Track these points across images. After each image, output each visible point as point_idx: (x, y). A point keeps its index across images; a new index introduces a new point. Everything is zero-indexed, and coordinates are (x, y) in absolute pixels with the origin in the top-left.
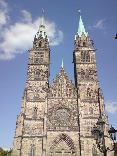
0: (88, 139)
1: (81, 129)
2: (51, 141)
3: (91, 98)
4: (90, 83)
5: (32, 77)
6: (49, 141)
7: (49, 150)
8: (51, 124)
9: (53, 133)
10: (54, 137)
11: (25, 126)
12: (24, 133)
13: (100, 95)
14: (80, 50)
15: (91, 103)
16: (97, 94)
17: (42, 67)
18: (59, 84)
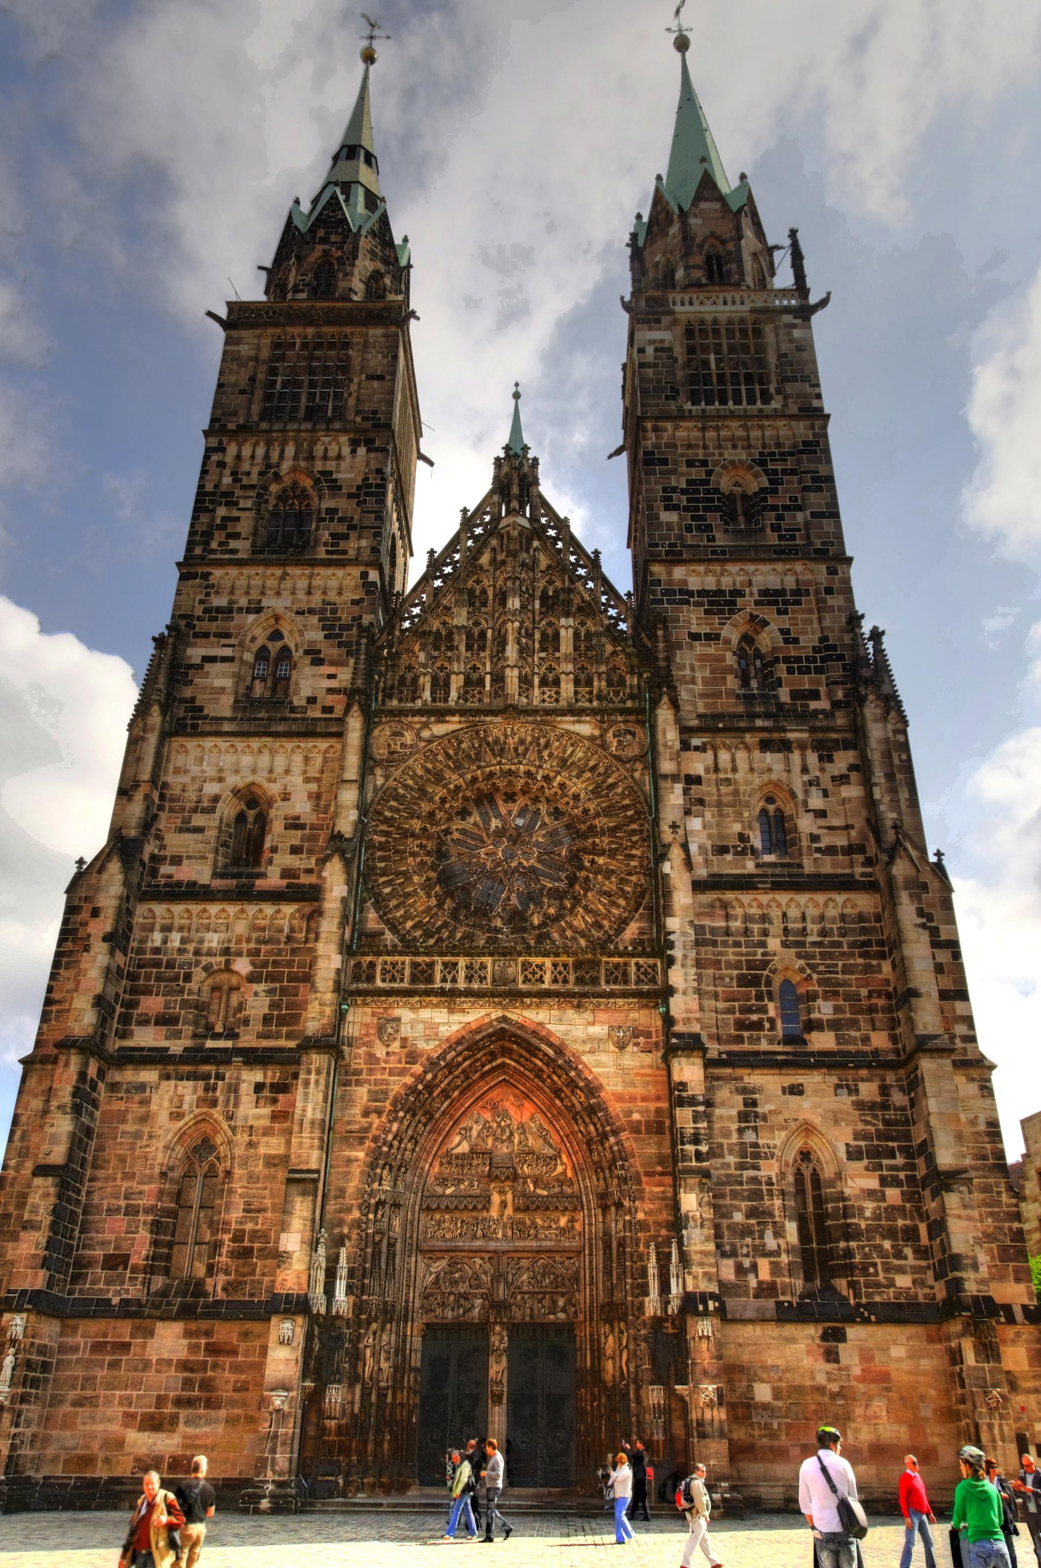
0: (755, 1078)
2: (374, 1096)
3: (780, 706)
4: (767, 575)
5: (236, 536)
8: (389, 936)
9: (405, 1014)
10: (412, 1057)
11: (140, 951)
12: (125, 1019)
14: (678, 308)
15: (786, 746)
17: (333, 452)
18: (484, 592)
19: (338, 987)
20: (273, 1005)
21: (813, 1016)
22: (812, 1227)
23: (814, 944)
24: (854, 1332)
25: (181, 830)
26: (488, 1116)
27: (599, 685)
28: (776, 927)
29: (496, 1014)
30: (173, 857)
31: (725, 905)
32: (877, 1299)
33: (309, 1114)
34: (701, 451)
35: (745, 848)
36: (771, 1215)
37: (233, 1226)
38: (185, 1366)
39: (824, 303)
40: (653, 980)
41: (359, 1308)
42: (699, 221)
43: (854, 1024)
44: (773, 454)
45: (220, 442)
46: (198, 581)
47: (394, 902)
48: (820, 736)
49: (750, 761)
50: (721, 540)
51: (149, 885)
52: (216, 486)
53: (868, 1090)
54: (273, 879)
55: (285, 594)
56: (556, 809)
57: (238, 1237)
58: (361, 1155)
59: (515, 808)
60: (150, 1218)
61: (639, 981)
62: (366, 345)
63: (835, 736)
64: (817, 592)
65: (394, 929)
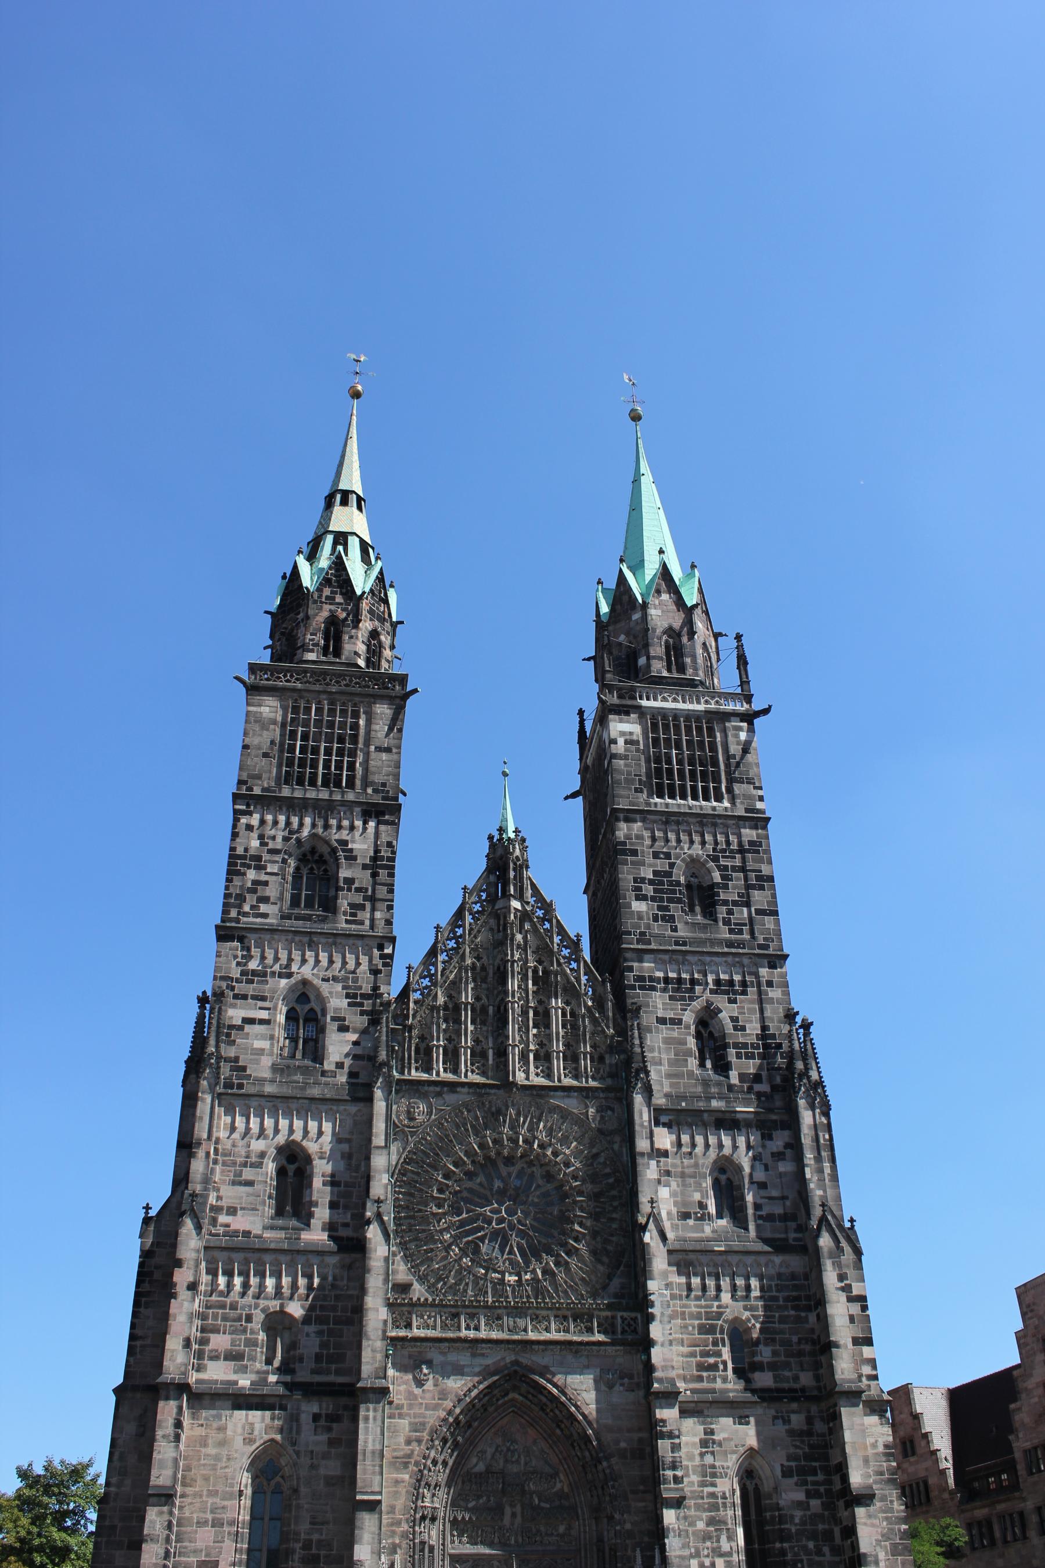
2: (416, 1427)
3: (731, 1088)
5: (265, 900)
6: (404, 1423)
7: (401, 1503)
8: (416, 1286)
12: (200, 1355)
13: (799, 1065)
14: (644, 703)
19: (385, 1337)
20: (323, 1345)
21: (757, 1359)
22: (754, 1532)
25: (234, 1183)
26: (499, 1441)
30: (229, 1208)
33: (370, 1447)
35: (703, 1215)
36: (726, 1523)
37: (303, 1536)
39: (766, 711)
40: (635, 1331)
42: (659, 612)
43: (787, 1365)
44: (724, 851)
51: (211, 1234)
52: (246, 850)
53: (797, 1420)
56: (548, 1172)
57: (307, 1545)
58: (407, 1477)
59: (514, 1170)
61: (624, 1332)
63: (774, 1117)
65: (422, 1279)
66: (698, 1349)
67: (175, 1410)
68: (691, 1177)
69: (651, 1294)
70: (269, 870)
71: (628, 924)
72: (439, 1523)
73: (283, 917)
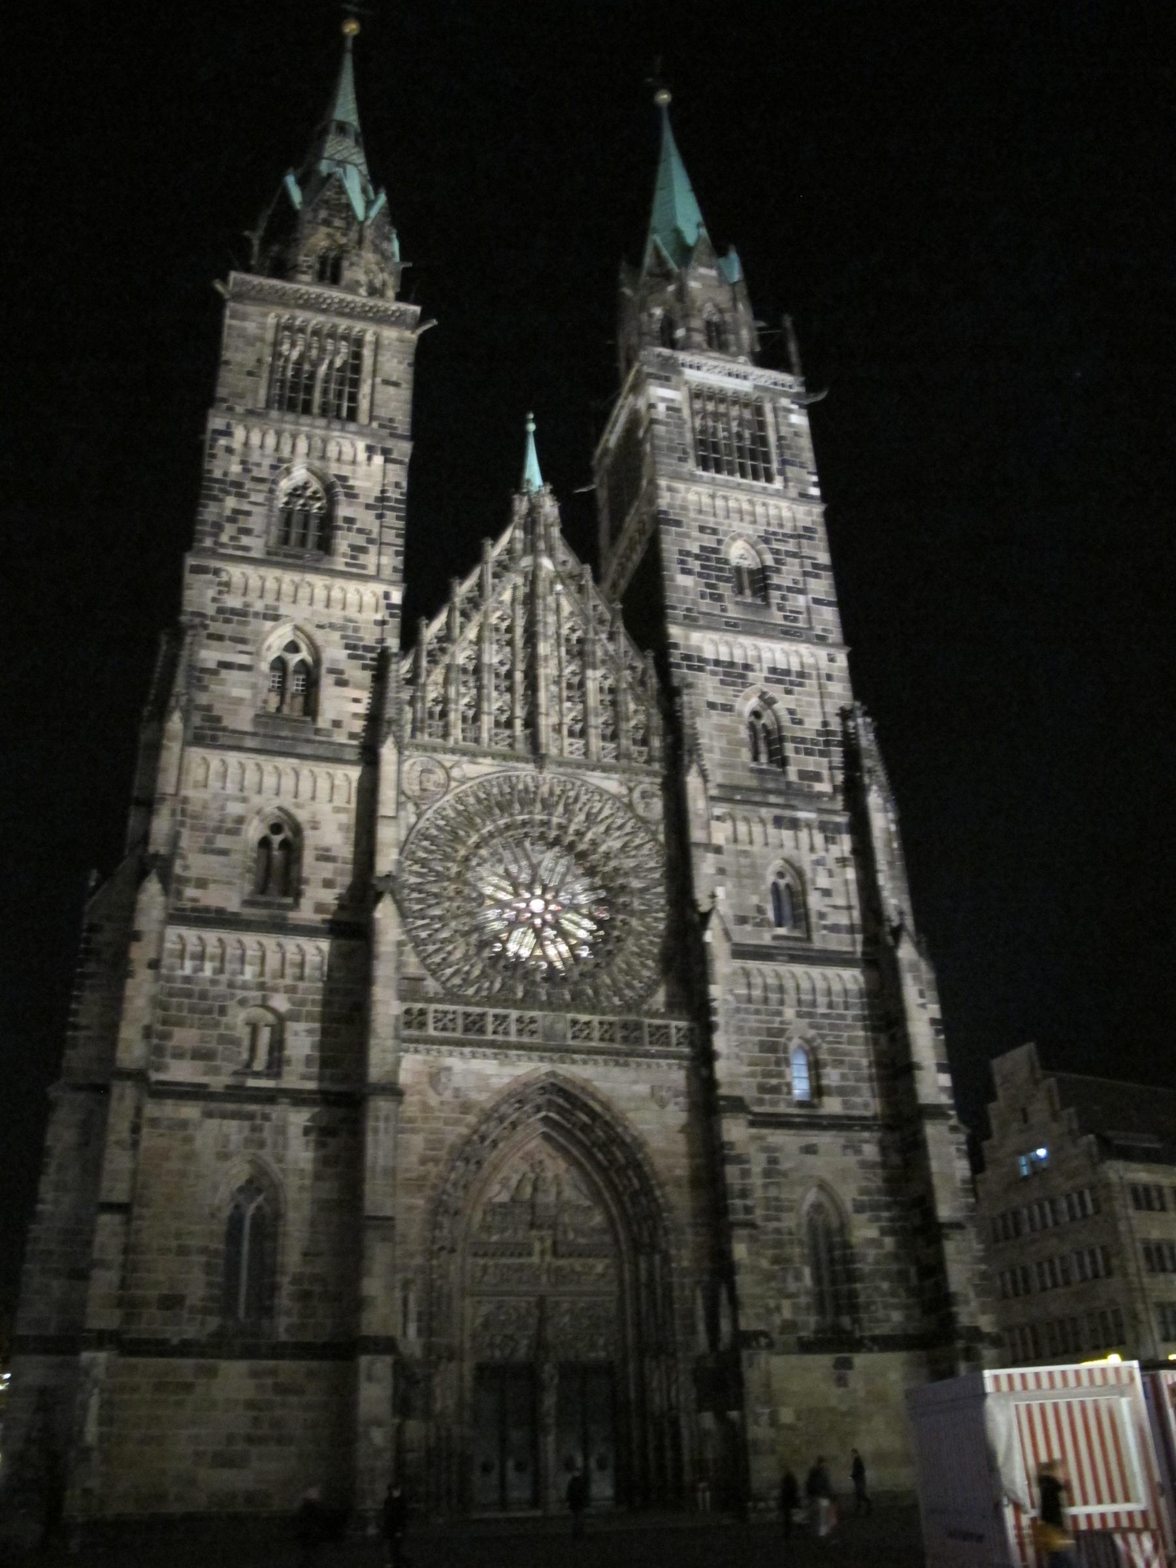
1: (720, 1042)
2: (433, 1145)
3: (789, 784)
5: (247, 532)
10: (466, 1107)
12: (159, 1051)
15: (794, 824)
16: (837, 757)
21: (825, 1082)
23: (824, 1016)
24: (860, 1360)
25: (205, 851)
27: (625, 742)
28: (791, 997)
29: (545, 1067)
31: (747, 974)
32: (877, 1332)
34: (712, 519)
35: (762, 920)
38: (251, 1405)
41: (428, 1349)
44: (774, 533)
45: (228, 425)
46: (210, 576)
47: (431, 948)
48: (826, 817)
49: (766, 835)
50: (733, 612)
52: (225, 474)
54: (306, 913)
55: (303, 604)
58: (421, 1202)
60: (203, 1259)
62: (377, 345)
64: (819, 677)
65: (434, 973)
66: (759, 1068)
67: (131, 1113)
68: (746, 877)
69: (714, 1000)
70: (253, 499)
71: (672, 597)
72: (457, 1258)
73: (268, 553)
